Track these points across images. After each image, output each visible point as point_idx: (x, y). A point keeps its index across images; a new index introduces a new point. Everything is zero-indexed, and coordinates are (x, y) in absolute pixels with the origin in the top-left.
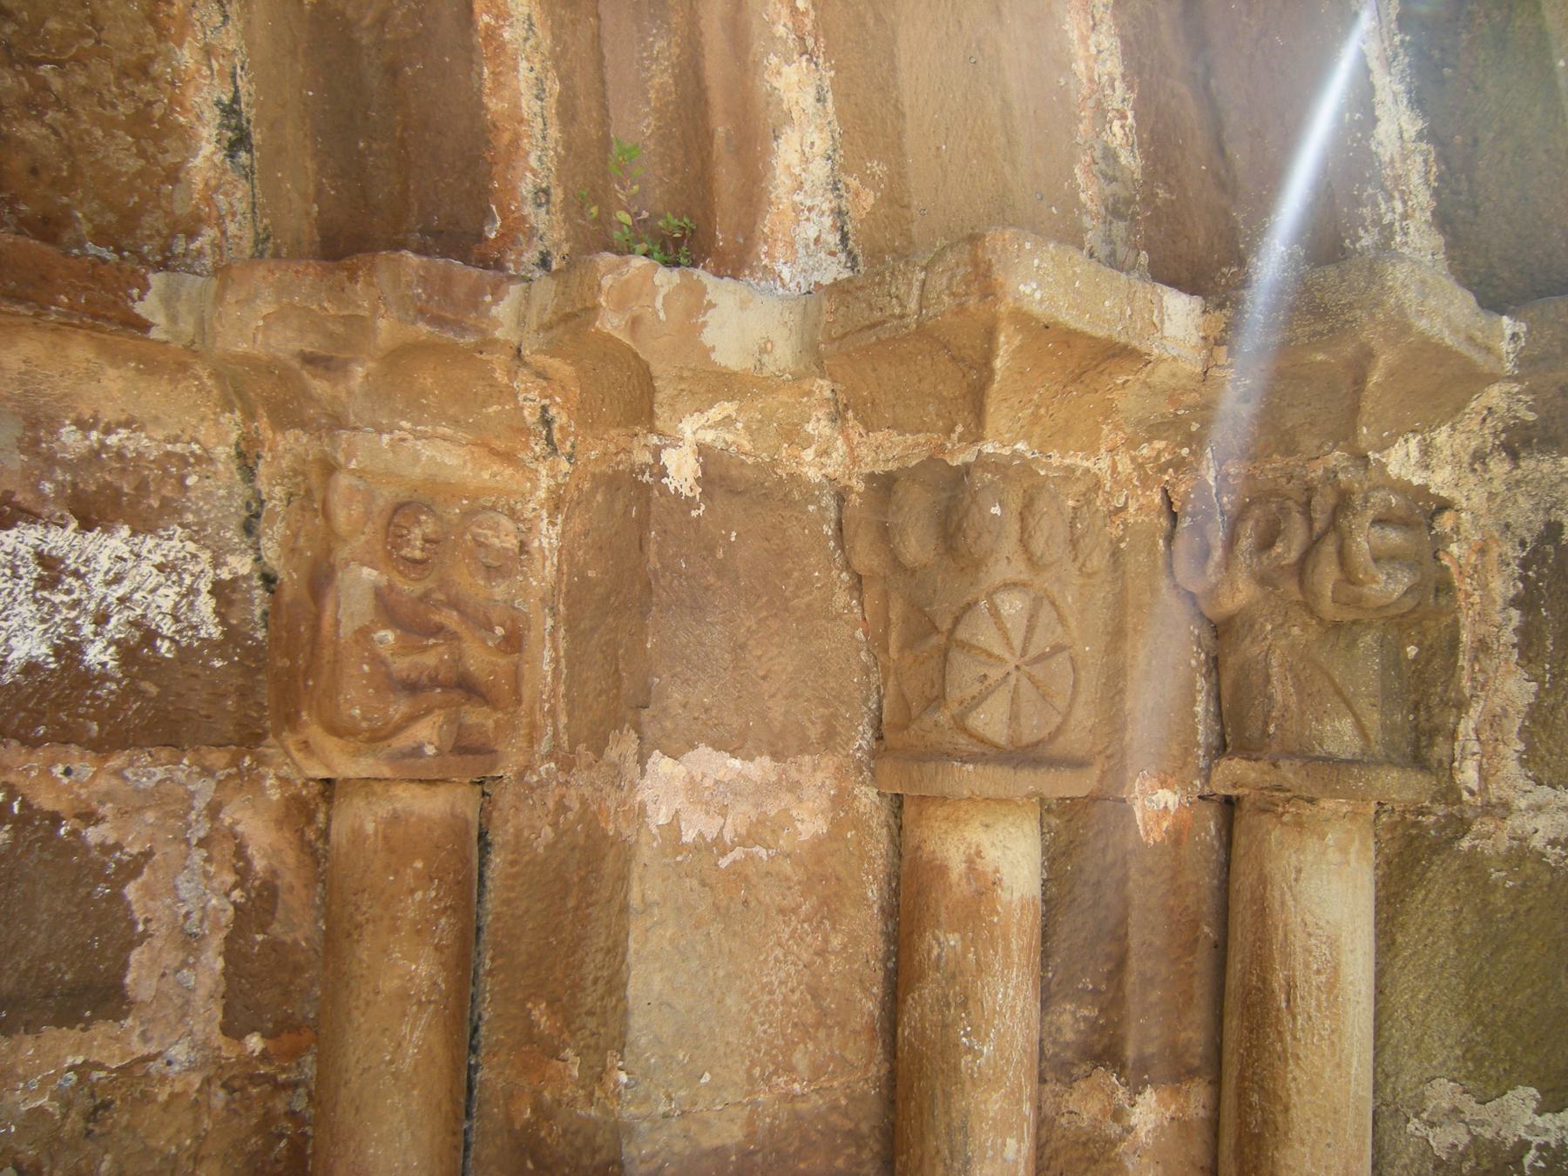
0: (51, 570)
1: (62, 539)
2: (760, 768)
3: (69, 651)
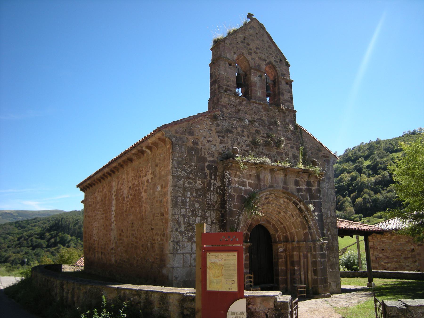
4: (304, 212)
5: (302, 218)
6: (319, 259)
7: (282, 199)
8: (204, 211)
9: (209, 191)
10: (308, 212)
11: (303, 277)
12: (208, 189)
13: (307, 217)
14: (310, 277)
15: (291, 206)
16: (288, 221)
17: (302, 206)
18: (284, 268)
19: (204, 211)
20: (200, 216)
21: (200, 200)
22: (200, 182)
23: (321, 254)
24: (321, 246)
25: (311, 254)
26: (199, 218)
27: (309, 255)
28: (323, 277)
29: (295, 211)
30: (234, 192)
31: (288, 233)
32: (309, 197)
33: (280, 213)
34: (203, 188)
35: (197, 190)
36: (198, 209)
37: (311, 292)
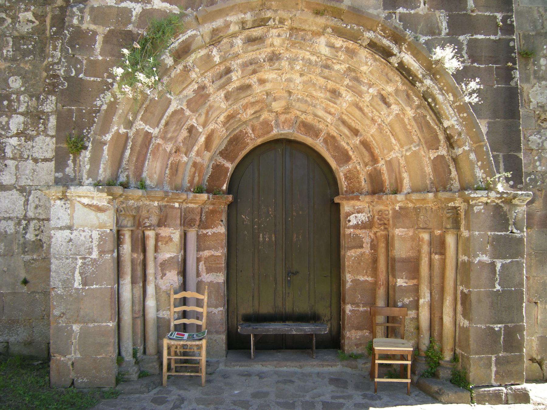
0: (356, 217)
1: (356, 215)
2: (406, 230)
3: (358, 223)
4: (422, 82)
5: (418, 107)
6: (485, 258)
7: (322, 40)
8: (38, 98)
9: (58, 39)
10: (434, 79)
11: (424, 315)
12: (55, 33)
13: (434, 99)
14: (447, 320)
15: (367, 63)
16: (373, 120)
17: (408, 59)
18: (369, 279)
19: (38, 98)
20: (22, 114)
21: (28, 67)
22: (29, 15)
23: (497, 239)
24: (497, 207)
25: (458, 237)
26: (21, 119)
27: (450, 240)
28: (497, 327)
29: (389, 81)
30: (94, 21)
31: (382, 165)
32: (444, 25)
33: (340, 95)
34: (40, 31)
35: (19, 39)
36: (18, 93)
37: (445, 373)
